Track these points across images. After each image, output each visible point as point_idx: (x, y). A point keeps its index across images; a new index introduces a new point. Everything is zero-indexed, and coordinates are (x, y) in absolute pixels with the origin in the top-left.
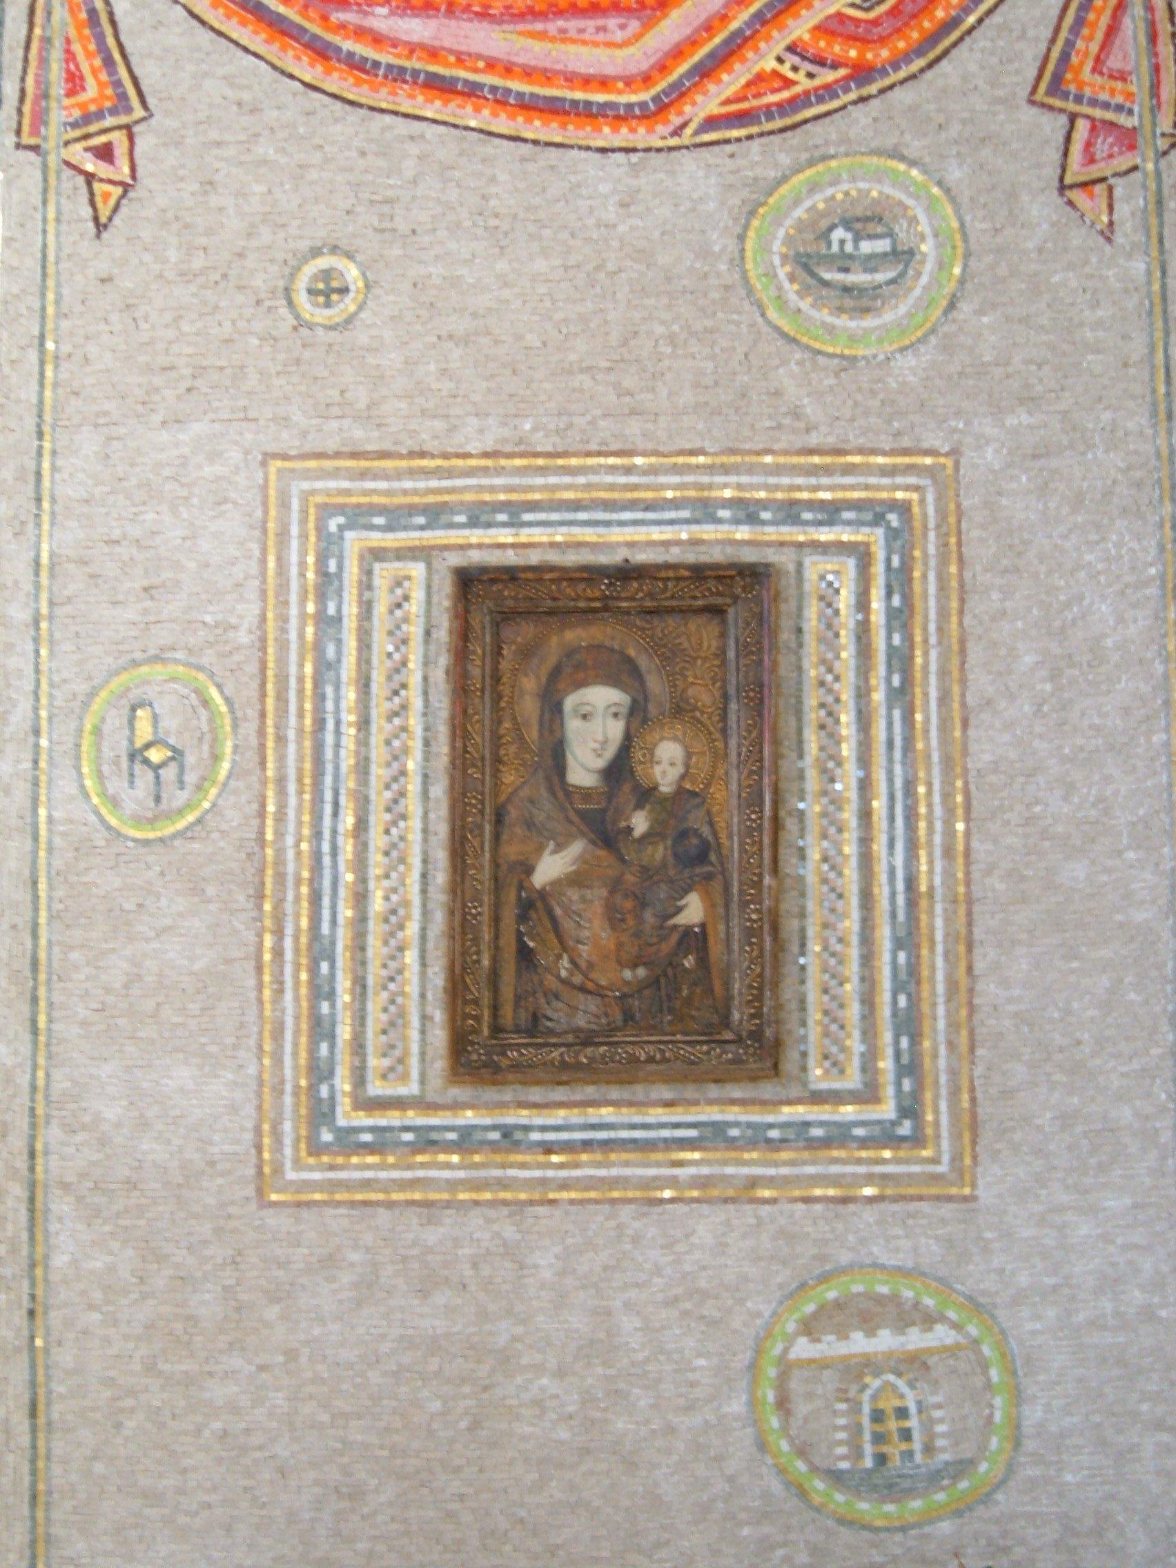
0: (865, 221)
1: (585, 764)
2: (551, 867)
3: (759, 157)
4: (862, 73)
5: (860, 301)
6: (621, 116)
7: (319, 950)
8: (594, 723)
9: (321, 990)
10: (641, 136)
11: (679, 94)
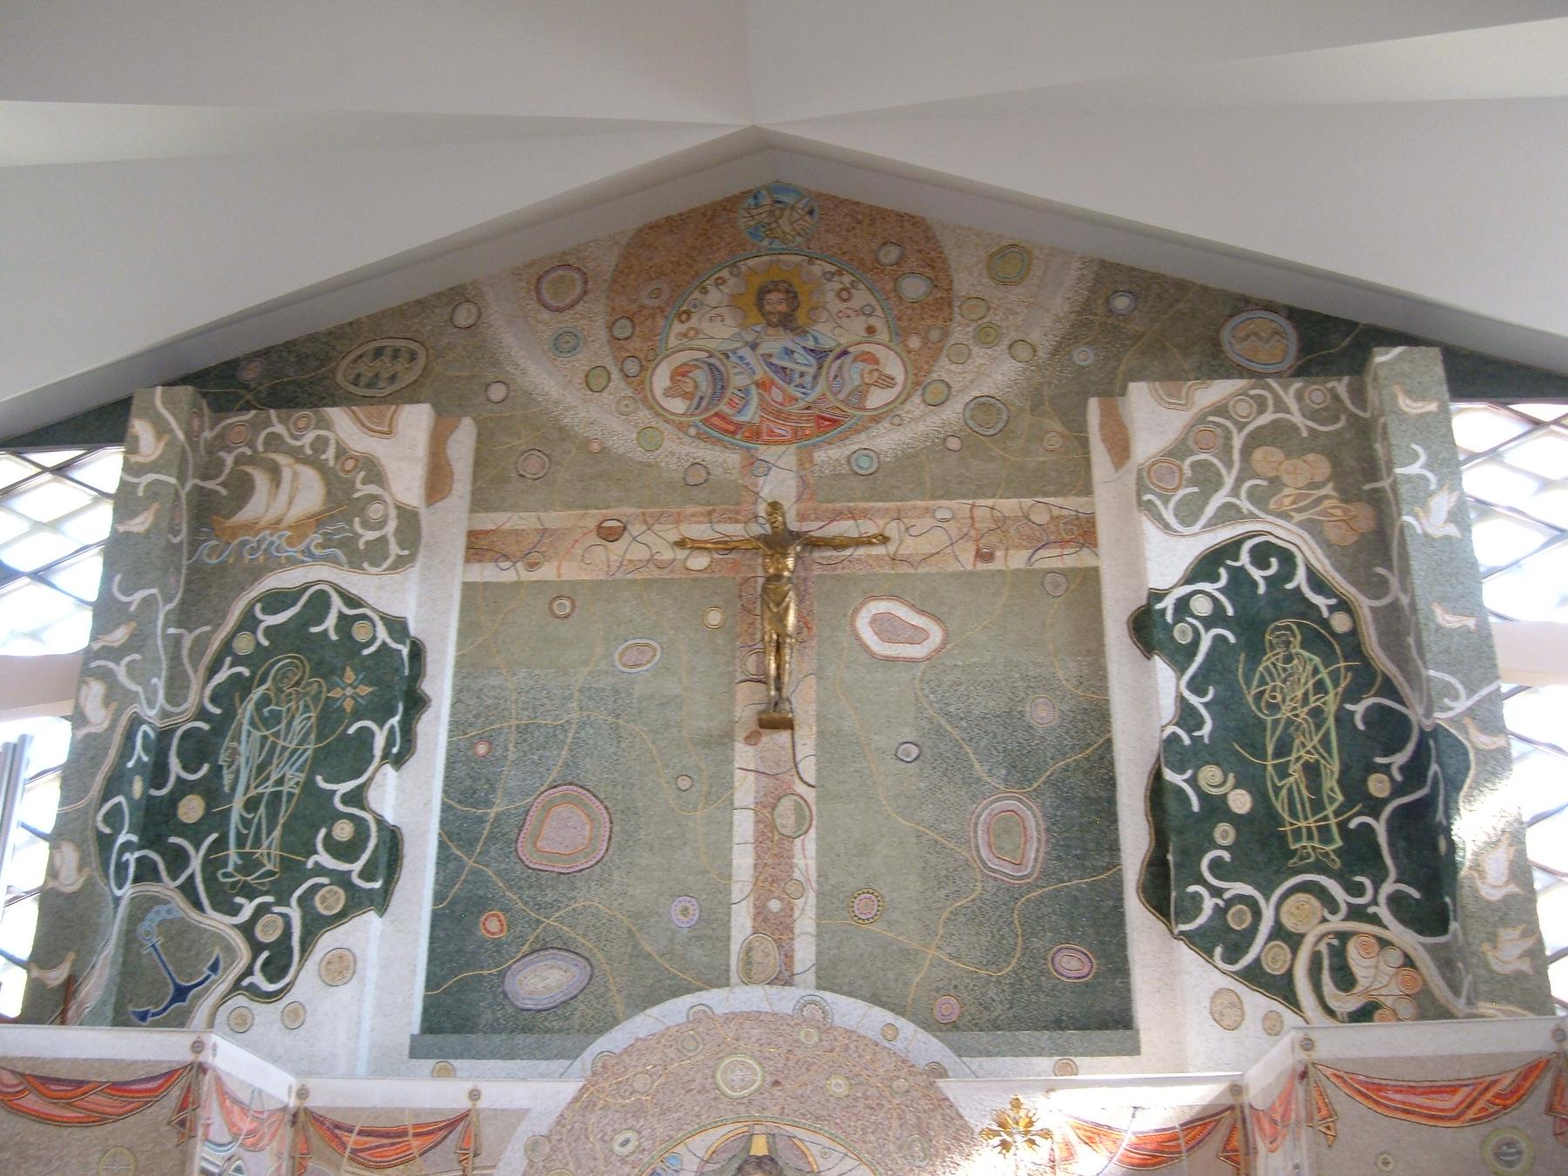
0: (1510, 1144)
3: (1484, 1129)
4: (1505, 1107)
5: (1510, 1164)
6: (1450, 1119)
10: (1456, 1124)
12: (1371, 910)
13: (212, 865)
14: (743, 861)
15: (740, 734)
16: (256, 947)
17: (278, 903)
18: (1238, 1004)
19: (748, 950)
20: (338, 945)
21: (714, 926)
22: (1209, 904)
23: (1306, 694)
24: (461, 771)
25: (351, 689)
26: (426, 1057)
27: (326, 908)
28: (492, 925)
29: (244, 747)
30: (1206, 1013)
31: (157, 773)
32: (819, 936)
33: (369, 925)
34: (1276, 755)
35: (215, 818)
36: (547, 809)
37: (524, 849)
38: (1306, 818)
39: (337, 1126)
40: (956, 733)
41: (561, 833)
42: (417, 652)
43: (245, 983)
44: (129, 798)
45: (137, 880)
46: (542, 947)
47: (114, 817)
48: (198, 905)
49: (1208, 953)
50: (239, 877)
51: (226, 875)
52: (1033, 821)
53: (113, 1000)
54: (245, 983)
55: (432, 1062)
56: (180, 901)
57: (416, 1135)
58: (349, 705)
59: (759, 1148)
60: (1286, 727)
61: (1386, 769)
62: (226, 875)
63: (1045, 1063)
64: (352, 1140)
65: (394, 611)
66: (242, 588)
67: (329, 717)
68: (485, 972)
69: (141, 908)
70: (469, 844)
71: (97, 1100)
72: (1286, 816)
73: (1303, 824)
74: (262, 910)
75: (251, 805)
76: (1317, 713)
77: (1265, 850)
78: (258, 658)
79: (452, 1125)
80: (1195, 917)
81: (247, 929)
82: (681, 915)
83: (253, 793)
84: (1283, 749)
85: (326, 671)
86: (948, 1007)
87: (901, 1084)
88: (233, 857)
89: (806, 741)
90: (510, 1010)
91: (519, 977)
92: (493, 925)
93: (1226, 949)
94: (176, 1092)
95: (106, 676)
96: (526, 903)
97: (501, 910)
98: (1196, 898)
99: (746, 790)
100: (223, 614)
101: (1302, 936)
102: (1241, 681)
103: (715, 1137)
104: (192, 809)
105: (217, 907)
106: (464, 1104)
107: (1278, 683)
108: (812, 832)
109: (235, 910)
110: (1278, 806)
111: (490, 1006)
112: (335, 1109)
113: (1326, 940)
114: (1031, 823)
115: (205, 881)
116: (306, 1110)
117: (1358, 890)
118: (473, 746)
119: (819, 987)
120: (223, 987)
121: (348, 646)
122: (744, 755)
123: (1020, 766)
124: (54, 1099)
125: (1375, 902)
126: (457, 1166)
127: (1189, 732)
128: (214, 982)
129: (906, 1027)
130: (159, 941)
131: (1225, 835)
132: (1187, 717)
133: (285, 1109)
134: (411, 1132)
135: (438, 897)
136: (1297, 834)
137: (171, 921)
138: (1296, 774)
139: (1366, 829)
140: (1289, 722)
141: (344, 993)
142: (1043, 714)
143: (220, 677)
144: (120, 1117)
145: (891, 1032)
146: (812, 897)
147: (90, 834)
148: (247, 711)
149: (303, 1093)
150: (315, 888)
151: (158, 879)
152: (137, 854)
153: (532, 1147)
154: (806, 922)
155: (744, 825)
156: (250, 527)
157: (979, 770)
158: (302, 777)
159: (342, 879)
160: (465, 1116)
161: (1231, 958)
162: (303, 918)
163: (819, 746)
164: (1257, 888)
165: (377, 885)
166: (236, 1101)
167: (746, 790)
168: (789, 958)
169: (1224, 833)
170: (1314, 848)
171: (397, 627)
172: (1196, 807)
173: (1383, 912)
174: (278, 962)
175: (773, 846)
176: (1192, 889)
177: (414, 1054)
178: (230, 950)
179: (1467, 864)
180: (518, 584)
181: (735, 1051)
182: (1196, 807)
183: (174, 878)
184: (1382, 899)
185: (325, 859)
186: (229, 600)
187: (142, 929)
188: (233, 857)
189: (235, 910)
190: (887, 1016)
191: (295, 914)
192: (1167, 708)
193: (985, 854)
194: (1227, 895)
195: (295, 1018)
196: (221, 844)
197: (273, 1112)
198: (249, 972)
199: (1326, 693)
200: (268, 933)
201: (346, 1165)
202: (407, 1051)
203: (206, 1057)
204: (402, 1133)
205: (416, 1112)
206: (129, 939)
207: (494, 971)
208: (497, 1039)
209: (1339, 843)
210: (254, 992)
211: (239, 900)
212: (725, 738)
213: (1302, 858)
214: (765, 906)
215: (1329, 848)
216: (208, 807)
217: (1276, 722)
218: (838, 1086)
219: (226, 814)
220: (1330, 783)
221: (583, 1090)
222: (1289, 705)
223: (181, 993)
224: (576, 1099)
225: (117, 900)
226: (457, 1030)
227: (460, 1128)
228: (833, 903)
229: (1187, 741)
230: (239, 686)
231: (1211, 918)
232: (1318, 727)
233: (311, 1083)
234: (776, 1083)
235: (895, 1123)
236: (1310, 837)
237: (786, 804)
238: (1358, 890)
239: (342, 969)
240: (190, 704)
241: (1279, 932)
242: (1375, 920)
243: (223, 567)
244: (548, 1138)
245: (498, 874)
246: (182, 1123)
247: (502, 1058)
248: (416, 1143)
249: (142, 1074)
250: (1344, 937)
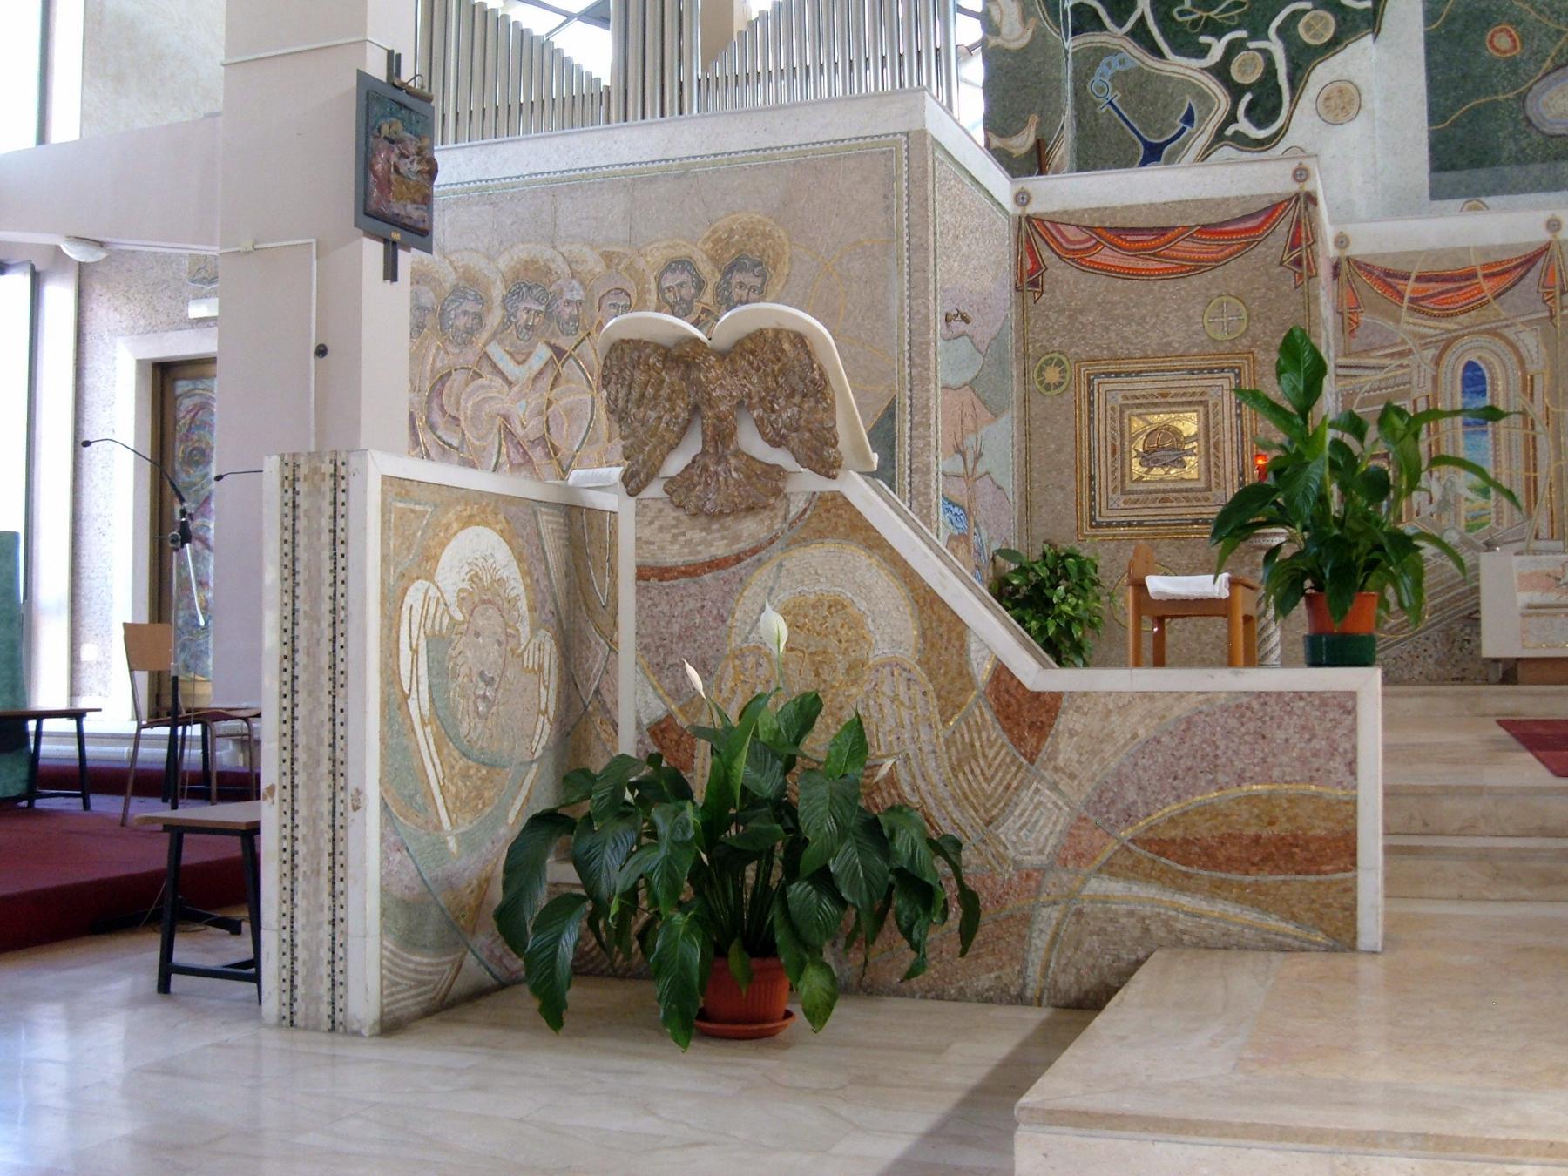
16: (1236, 91)
17: (1253, 37)
20: (1334, 77)
26: (1450, 197)
27: (1314, 37)
28: (1502, 41)
39: (1388, 273)
43: (1229, 131)
48: (1157, 52)
50: (1198, 14)
51: (1182, 13)
54: (1229, 131)
55: (1460, 202)
57: (1486, 276)
62: (1182, 13)
64: (1409, 288)
69: (1088, 62)
71: (1186, 246)
74: (1233, 49)
79: (1530, 261)
81: (1221, 71)
90: (1537, 138)
91: (1544, 98)
92: (1503, 42)
94: (1283, 228)
96: (1541, 12)
97: (1510, 23)
105: (1177, 50)
106: (1543, 236)
111: (1511, 136)
112: (1384, 256)
115: (1158, 22)
116: (1348, 259)
120: (1203, 140)
124: (1135, 251)
126: (1540, 306)
128: (1191, 135)
130: (1116, 97)
134: (1480, 274)
137: (1126, 73)
141: (1353, 130)
144: (1218, 263)
150: (1296, 16)
151: (1102, 27)
160: (1544, 250)
162: (1287, 51)
174: (1266, 104)
177: (1436, 193)
178: (1203, 97)
183: (1121, 25)
187: (1094, 84)
189: (1203, 51)
198: (1232, 118)
200: (1246, 71)
201: (1405, 316)
202: (1427, 193)
204: (1470, 275)
205: (1485, 251)
207: (1511, 95)
208: (1536, 169)
211: (1203, 39)
226: (1476, 162)
227: (1540, 264)
233: (1349, 229)
239: (1343, 104)
246: (1298, 262)
247: (1547, 189)
248: (1487, 286)
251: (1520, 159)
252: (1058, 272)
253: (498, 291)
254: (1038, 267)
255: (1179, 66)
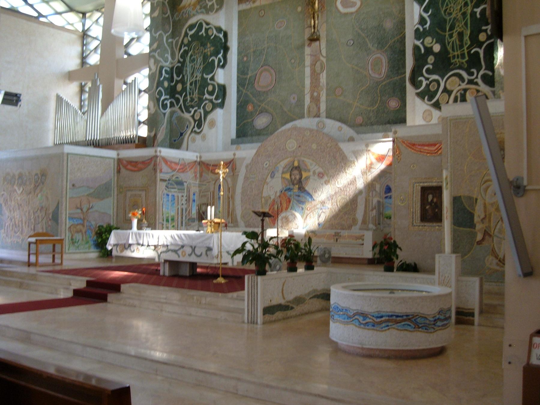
1: (430, 199)
2: (427, 207)
7: (413, 212)
8: (430, 197)
9: (413, 215)
11: (437, 152)
12: (475, 80)
13: (185, 101)
14: (308, 82)
15: (306, 45)
16: (195, 121)
18: (431, 115)
19: (309, 108)
21: (300, 102)
22: (424, 83)
23: (461, 7)
24: (241, 66)
25: (210, 49)
28: (250, 108)
29: (188, 69)
30: (421, 118)
31: (171, 79)
32: (327, 101)
33: (219, 112)
34: (450, 30)
35: (184, 89)
36: (261, 74)
37: (256, 85)
38: (457, 51)
40: (363, 35)
41: (264, 80)
42: (226, 35)
44: (163, 87)
45: (170, 107)
46: (261, 112)
47: (160, 94)
48: (183, 112)
49: (423, 98)
52: (384, 60)
53: (169, 137)
56: (179, 111)
58: (209, 54)
59: (296, 164)
60: (454, 20)
61: (486, 31)
63: (380, 135)
65: (217, 24)
66: (184, 25)
67: (205, 57)
68: (249, 120)
70: (243, 86)
71: (140, 166)
72: (451, 51)
73: (456, 53)
75: (191, 84)
76: (464, 14)
77: (443, 64)
78: (189, 44)
79: (230, 162)
80: (420, 88)
81: (193, 116)
82: (293, 99)
83: (191, 81)
84: (452, 28)
85: (204, 45)
86: (359, 120)
87: (329, 145)
88: (189, 99)
89: (323, 43)
93: (428, 97)
95: (154, 57)
98: (421, 82)
99: (308, 61)
100: (181, 33)
101: (452, 91)
102: (440, 6)
103: (285, 162)
104: (179, 87)
105: (186, 111)
106: (232, 157)
107: (452, 5)
108: (325, 71)
109: (190, 112)
110: (449, 49)
113: (459, 92)
114: (384, 61)
116: (202, 162)
117: (472, 74)
118: (243, 58)
119: (327, 117)
121: (208, 36)
122: (308, 50)
123: (381, 43)
125: (477, 77)
127: (423, 26)
129: (344, 126)
131: (431, 60)
132: (422, 21)
133: (196, 162)
135: (238, 102)
136: (454, 57)
138: (455, 35)
139: (477, 53)
140: (455, 18)
141: (214, 130)
142: (389, 25)
143: (182, 51)
145: (340, 129)
146: (325, 90)
147: (155, 98)
148: (188, 59)
149: (200, 157)
150: (205, 104)
152: (169, 101)
153: (247, 167)
154: (323, 98)
155: (308, 71)
156: (184, 7)
157: (370, 45)
158: (201, 75)
159: (211, 101)
160: (233, 160)
161: (430, 99)
163: (327, 45)
164: (440, 76)
165: (220, 101)
166: (171, 162)
167: (308, 61)
168: (319, 109)
169: (431, 59)
170: (459, 61)
171: (219, 30)
172: (423, 51)
173: (479, 81)
175: (315, 76)
176: (420, 78)
178: (190, 123)
179: (498, 64)
180: (251, 8)
181: (290, 139)
182: (423, 51)
184: (479, 76)
185: (207, 96)
186: (182, 29)
187: (173, 119)
188: (189, 99)
189: (190, 112)
190: (338, 124)
191: (202, 111)
192: (416, 19)
193: (370, 72)
194: (430, 80)
195: (204, 138)
196: (186, 95)
197: (188, 164)
198: (194, 127)
199: (468, 6)
200: (197, 117)
203: (158, 154)
206: (170, 122)
209: (467, 58)
210: (195, 132)
212: (302, 46)
213: (454, 65)
214: (313, 94)
215: (464, 61)
216: (183, 86)
217: (450, 19)
218: (314, 146)
219: (186, 87)
220: (466, 38)
221: (257, 151)
222: (455, 12)
223: (181, 134)
224: (256, 154)
225: (164, 114)
228: (330, 91)
229: (421, 29)
230: (186, 52)
231: (425, 88)
232: (464, 19)
233: (202, 155)
234: (300, 146)
235: (328, 156)
236: (458, 57)
237: (318, 64)
238: (472, 74)
240: (176, 59)
241: (445, 90)
242: (476, 84)
243: (179, 20)
244: (250, 164)
245: (251, 93)
249: (147, 159)
250: (465, 90)
251: (252, 135)
252: (123, 170)
253: (17, 177)
254: (120, 169)
255: (187, 116)
